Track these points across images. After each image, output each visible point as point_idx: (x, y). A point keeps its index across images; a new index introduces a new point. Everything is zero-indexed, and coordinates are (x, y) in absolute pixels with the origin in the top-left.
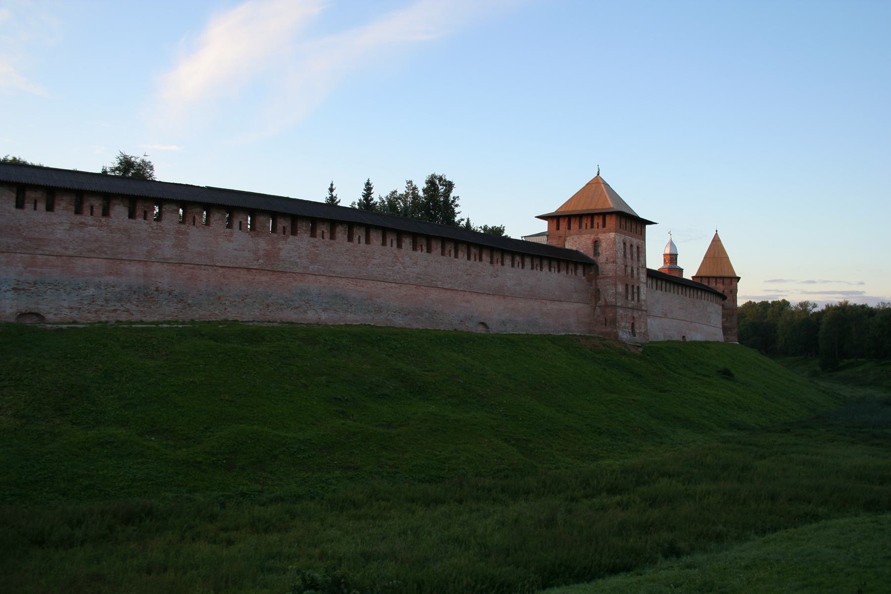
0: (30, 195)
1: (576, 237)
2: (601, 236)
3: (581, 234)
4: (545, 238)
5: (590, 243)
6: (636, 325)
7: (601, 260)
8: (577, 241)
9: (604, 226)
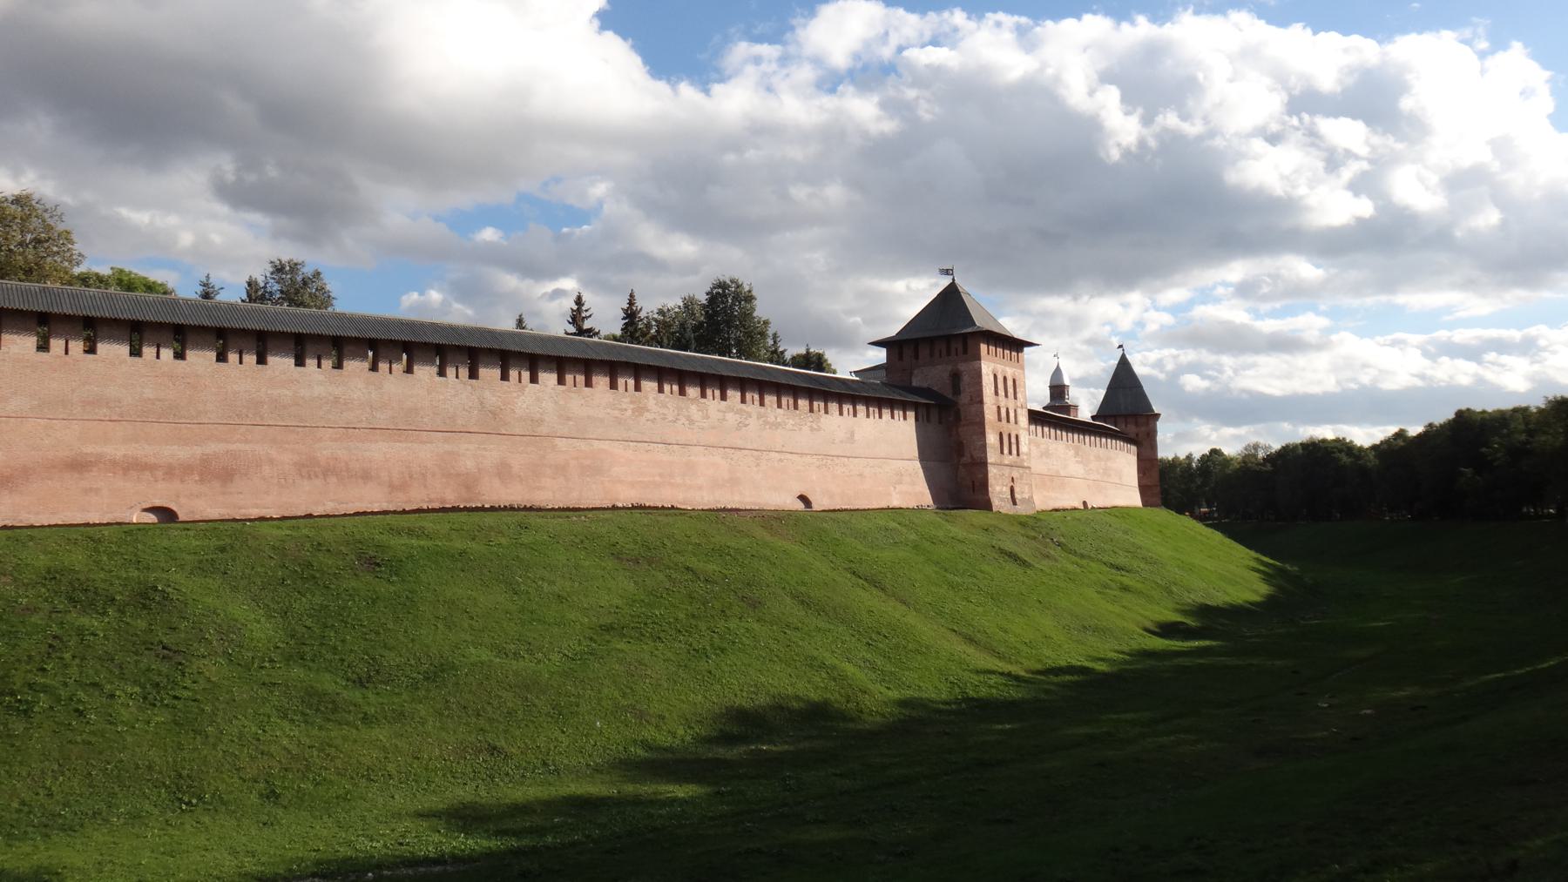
0: (309, 347)
2: (962, 367)
4: (883, 373)
6: (1017, 490)
8: (932, 375)
9: (965, 352)
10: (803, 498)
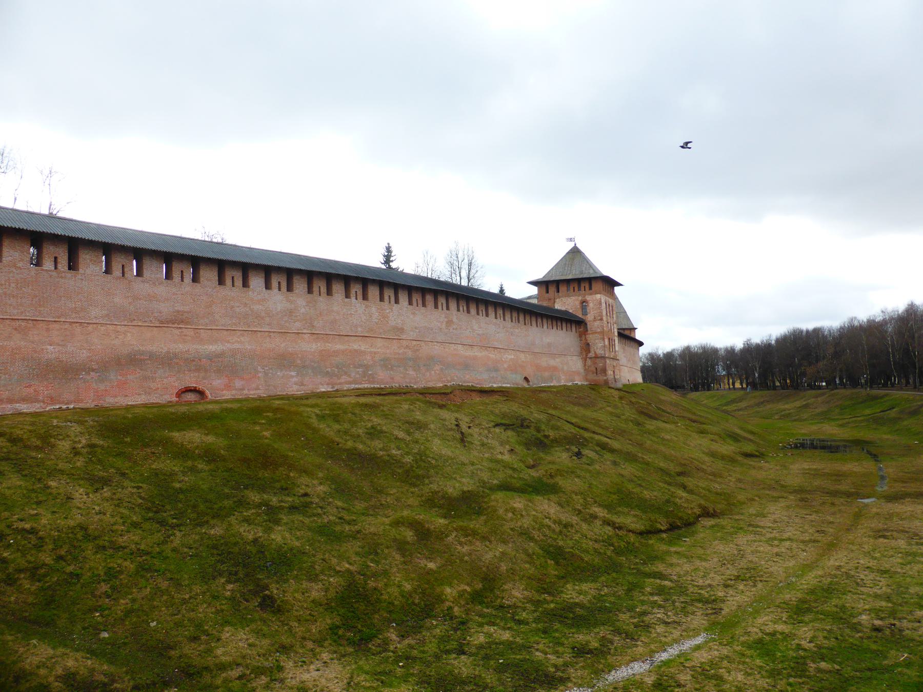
1: (564, 299)
2: (588, 298)
3: (569, 296)
5: (578, 303)
7: (589, 318)
8: (566, 303)
9: (590, 289)
10: (526, 379)
